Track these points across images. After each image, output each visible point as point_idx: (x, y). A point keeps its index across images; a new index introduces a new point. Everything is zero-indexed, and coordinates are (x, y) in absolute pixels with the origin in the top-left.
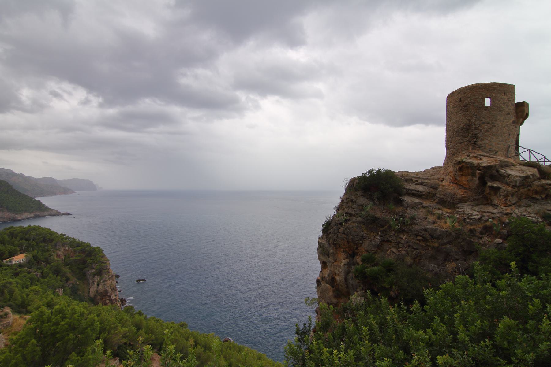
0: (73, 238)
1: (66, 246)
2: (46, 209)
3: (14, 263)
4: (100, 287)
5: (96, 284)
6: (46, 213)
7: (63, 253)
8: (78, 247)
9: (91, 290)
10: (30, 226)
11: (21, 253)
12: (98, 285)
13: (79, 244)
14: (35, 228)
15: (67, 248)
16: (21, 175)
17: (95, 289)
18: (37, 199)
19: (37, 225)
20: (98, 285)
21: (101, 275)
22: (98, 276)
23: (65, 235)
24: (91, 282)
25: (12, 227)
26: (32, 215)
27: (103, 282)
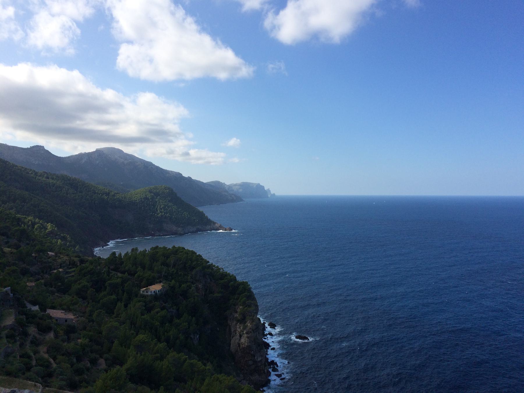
0: (218, 267)
3: (149, 293)
4: (243, 340)
5: (238, 334)
6: (208, 227)
8: (221, 279)
9: (232, 341)
10: (174, 247)
11: (160, 282)
12: (241, 336)
13: (225, 275)
14: (176, 251)
15: (209, 280)
16: (190, 178)
17: (237, 341)
18: (201, 209)
19: (181, 245)
20: (241, 336)
22: (240, 324)
23: (208, 262)
24: (233, 330)
26: (195, 229)
27: (247, 333)
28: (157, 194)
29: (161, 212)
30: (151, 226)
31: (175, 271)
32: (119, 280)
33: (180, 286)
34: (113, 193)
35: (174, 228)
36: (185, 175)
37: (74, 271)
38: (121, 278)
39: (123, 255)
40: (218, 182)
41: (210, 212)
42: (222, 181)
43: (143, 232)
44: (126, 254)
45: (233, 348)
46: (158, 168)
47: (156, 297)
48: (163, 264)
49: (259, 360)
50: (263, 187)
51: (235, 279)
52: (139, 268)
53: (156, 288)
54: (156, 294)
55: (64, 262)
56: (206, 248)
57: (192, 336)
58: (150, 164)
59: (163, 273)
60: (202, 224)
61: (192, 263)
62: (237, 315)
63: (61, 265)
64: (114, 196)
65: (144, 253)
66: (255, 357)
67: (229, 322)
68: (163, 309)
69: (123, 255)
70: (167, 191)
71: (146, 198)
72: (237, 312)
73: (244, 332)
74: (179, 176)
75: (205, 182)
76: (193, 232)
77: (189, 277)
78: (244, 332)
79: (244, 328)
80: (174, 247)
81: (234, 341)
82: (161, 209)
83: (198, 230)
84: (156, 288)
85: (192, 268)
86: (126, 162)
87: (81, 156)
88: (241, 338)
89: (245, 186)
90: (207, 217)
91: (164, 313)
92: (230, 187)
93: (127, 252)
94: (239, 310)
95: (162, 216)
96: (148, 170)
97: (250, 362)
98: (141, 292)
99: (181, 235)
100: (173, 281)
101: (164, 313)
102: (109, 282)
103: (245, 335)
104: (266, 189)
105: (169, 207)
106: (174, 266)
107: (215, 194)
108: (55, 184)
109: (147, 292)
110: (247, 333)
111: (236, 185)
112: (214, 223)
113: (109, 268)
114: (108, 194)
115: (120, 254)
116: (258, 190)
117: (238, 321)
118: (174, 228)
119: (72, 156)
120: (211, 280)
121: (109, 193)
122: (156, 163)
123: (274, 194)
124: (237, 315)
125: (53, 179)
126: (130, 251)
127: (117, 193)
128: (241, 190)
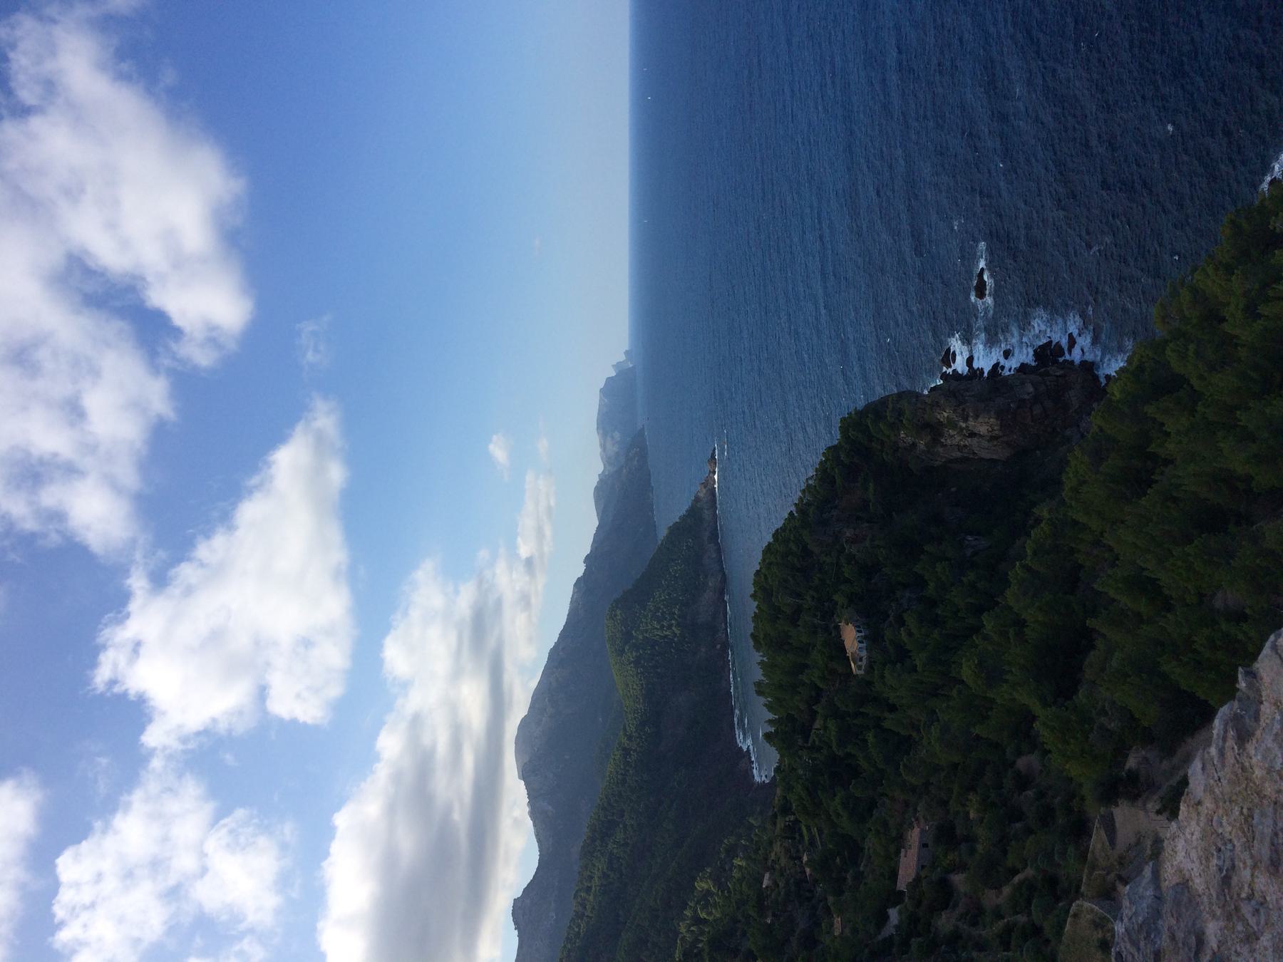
0: (803, 492)
2: (694, 512)
3: (864, 654)
4: (983, 430)
5: (968, 442)
6: (707, 514)
9: (985, 455)
10: (754, 596)
11: (838, 628)
13: (824, 474)
14: (763, 590)
16: (588, 559)
17: (985, 444)
18: (663, 532)
21: (940, 423)
22: (941, 435)
23: (791, 513)
24: (959, 454)
27: (966, 420)
28: (627, 636)
29: (670, 627)
31: (812, 592)
32: (832, 725)
33: (847, 581)
34: (624, 740)
35: (708, 596)
36: (580, 570)
37: (808, 828)
38: (825, 721)
39: (771, 716)
40: (598, 490)
41: (671, 509)
42: (594, 481)
43: (715, 668)
44: (770, 707)
45: (1001, 453)
46: (564, 635)
47: (872, 638)
48: (794, 620)
49: (1031, 389)
51: (832, 450)
52: (804, 678)
53: (851, 637)
54: (865, 637)
55: (787, 851)
56: (757, 517)
57: (969, 552)
58: (554, 653)
59: (816, 621)
61: (793, 554)
62: (922, 445)
63: (792, 858)
64: (630, 738)
65: (767, 667)
66: (1024, 400)
67: (937, 463)
68: (901, 622)
69: (771, 716)
70: (618, 612)
71: (637, 663)
72: (914, 445)
73: (964, 425)
74: (583, 586)
75: (597, 523)
76: (719, 551)
77: (828, 560)
78: (964, 425)
79: (954, 425)
80: (754, 596)
81: (984, 450)
82: (662, 627)
83: (714, 536)
84: (851, 637)
87: (536, 813)
88: (979, 433)
89: (606, 423)
90: (683, 518)
91: (911, 620)
92: (608, 460)
93: (765, 705)
94: (910, 440)
95: (678, 625)
96: (567, 659)
97: (1037, 410)
98: (862, 672)
99: (724, 580)
100: (836, 597)
101: (911, 620)
102: (834, 748)
103: (971, 423)
104: (613, 374)
105: (658, 609)
106: (799, 595)
107: (625, 498)
108: (604, 873)
109: (861, 659)
110: (966, 420)
111: (603, 447)
112: (697, 499)
113: (801, 748)
114: (626, 752)
115: (770, 722)
117: (936, 440)
118: (708, 596)
119: (537, 835)
120: (836, 507)
121: (624, 749)
123: (627, 353)
124: (922, 445)
125: (591, 878)
126: (762, 700)
127: (625, 729)
128: (617, 435)
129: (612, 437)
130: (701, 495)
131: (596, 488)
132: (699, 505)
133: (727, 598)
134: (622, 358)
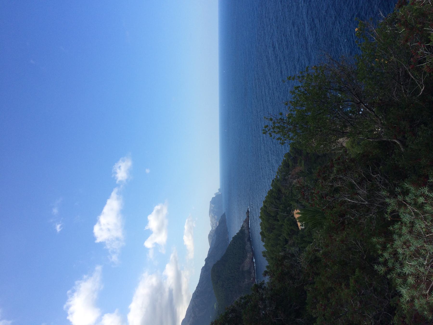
0: (278, 173)
1: (286, 177)
2: (242, 231)
7: (295, 179)
13: (286, 165)
15: (290, 176)
16: (207, 260)
18: (231, 239)
25: (262, 233)
26: (248, 243)
30: (246, 280)
35: (248, 260)
41: (235, 229)
50: (213, 198)
60: (244, 236)
74: (204, 269)
85: (279, 190)
86: (193, 315)
89: (211, 211)
111: (212, 222)
116: (215, 201)
120: (290, 174)
122: (193, 289)
123: (219, 190)
128: (216, 217)
129: (214, 218)
130: (244, 225)
131: (209, 235)
132: (243, 229)
133: (254, 260)
134: (218, 191)
